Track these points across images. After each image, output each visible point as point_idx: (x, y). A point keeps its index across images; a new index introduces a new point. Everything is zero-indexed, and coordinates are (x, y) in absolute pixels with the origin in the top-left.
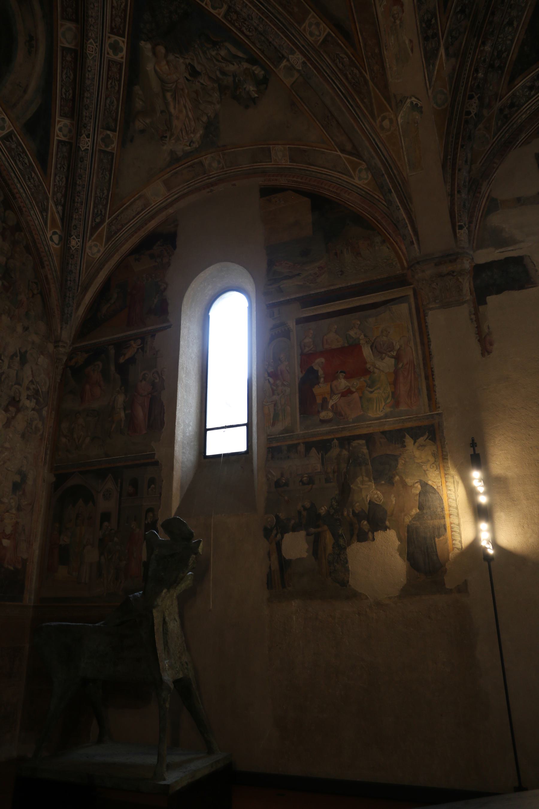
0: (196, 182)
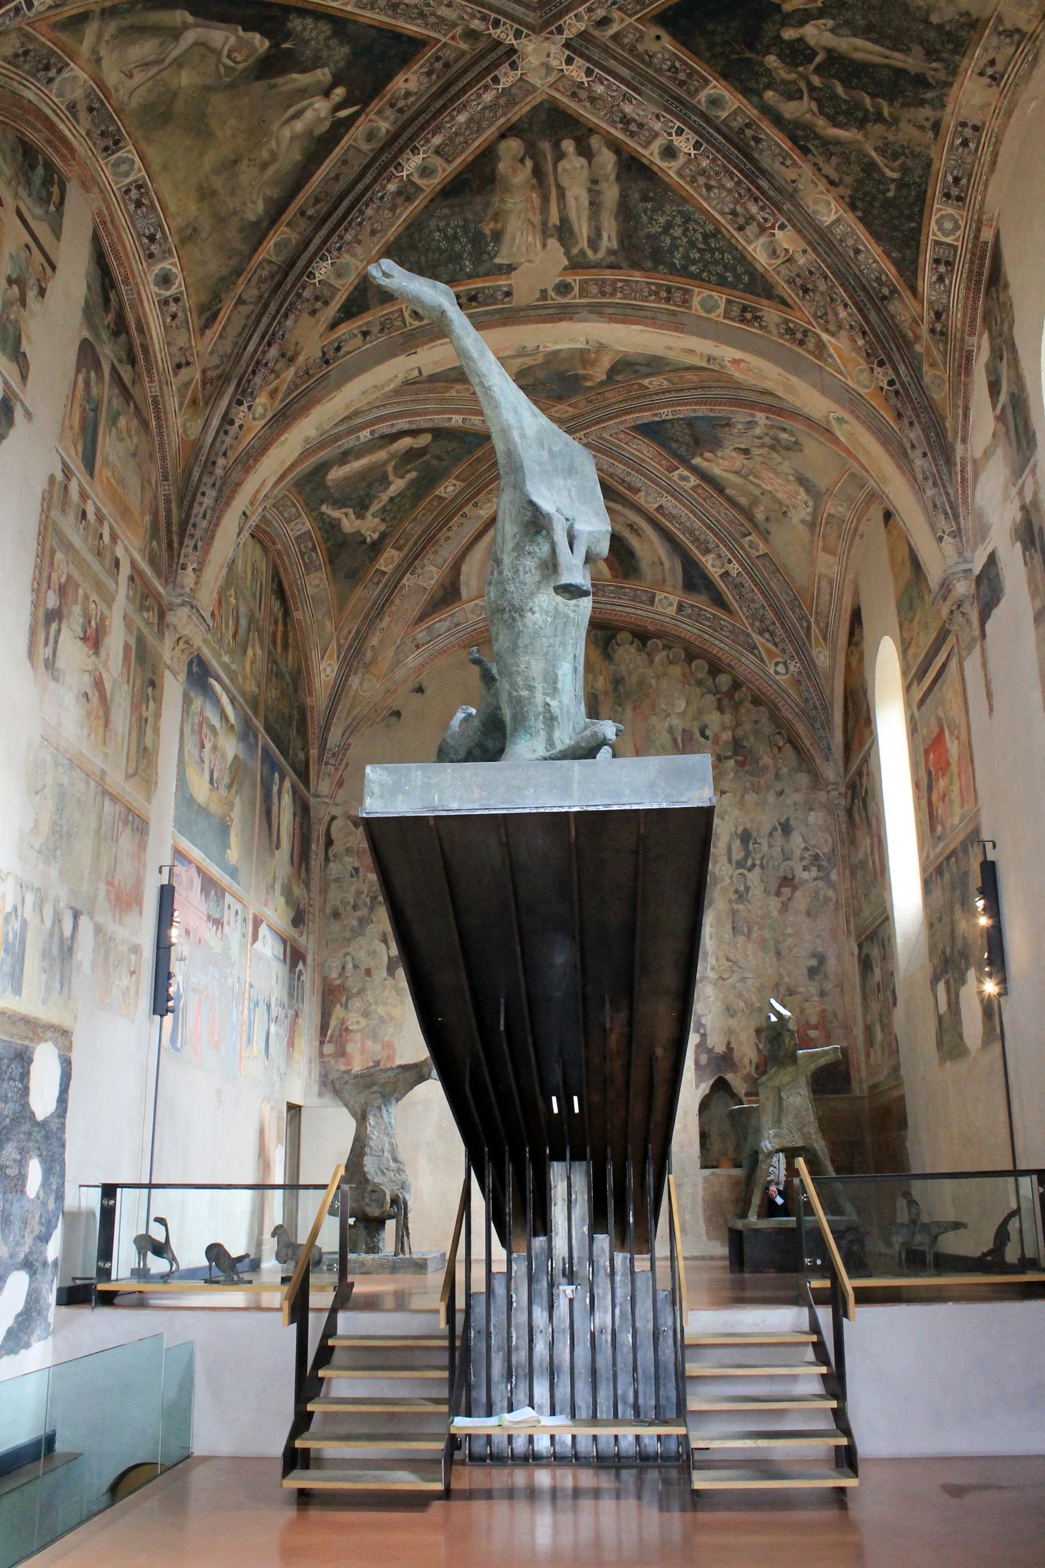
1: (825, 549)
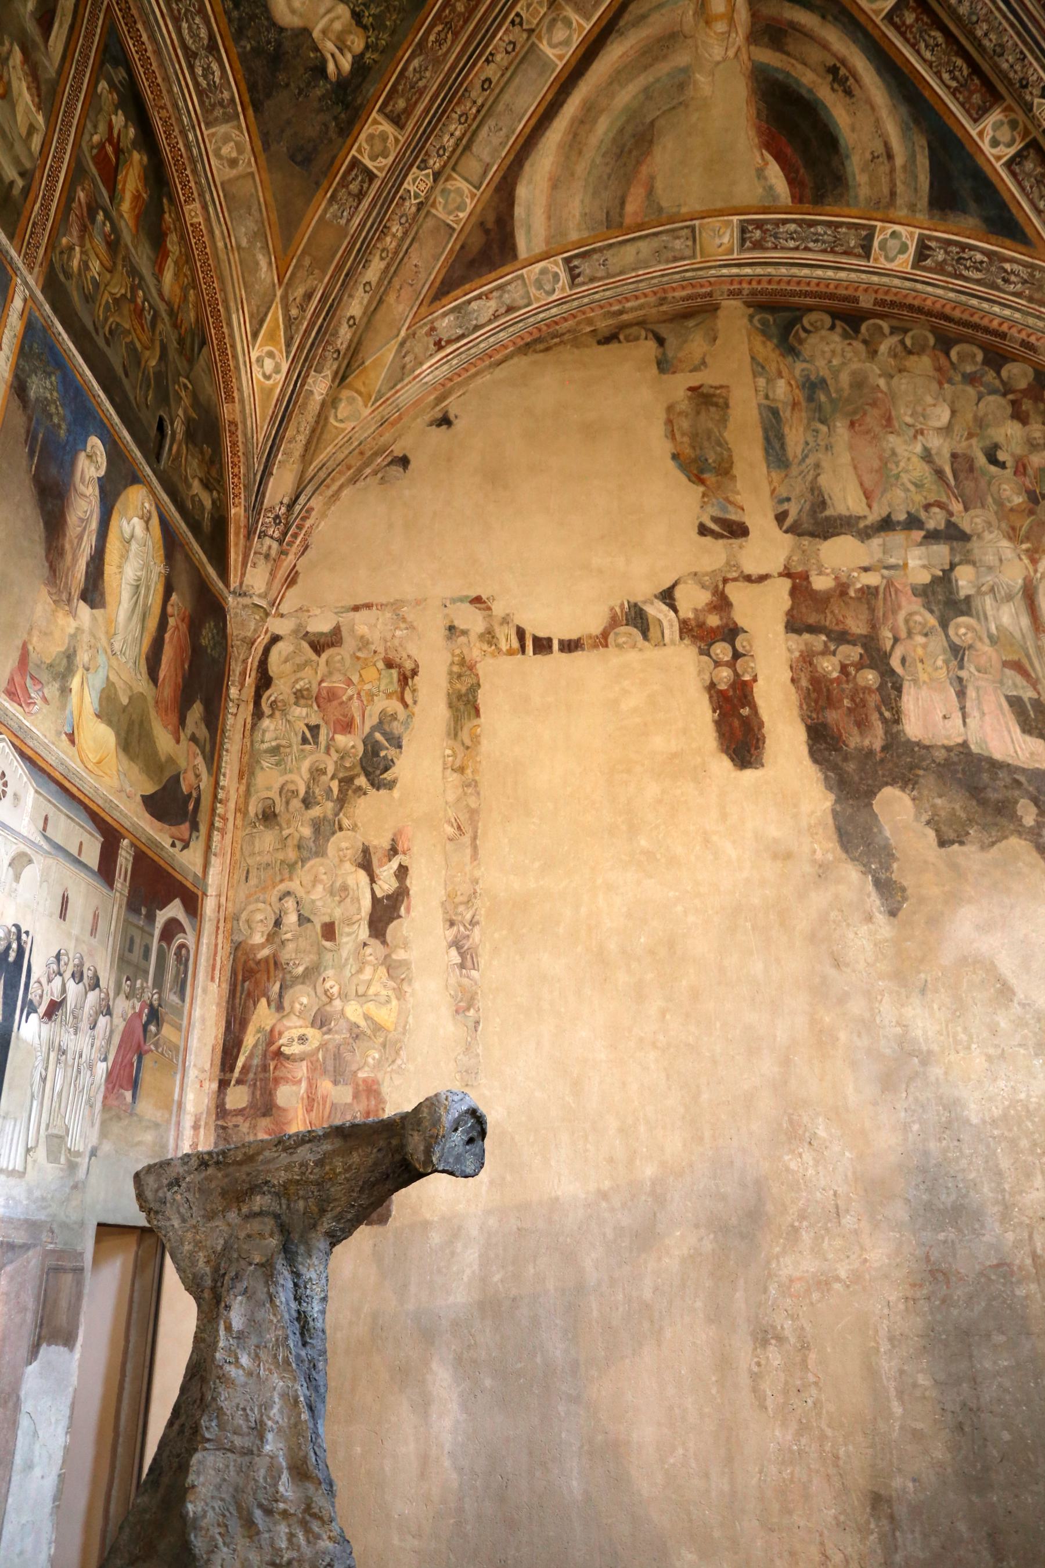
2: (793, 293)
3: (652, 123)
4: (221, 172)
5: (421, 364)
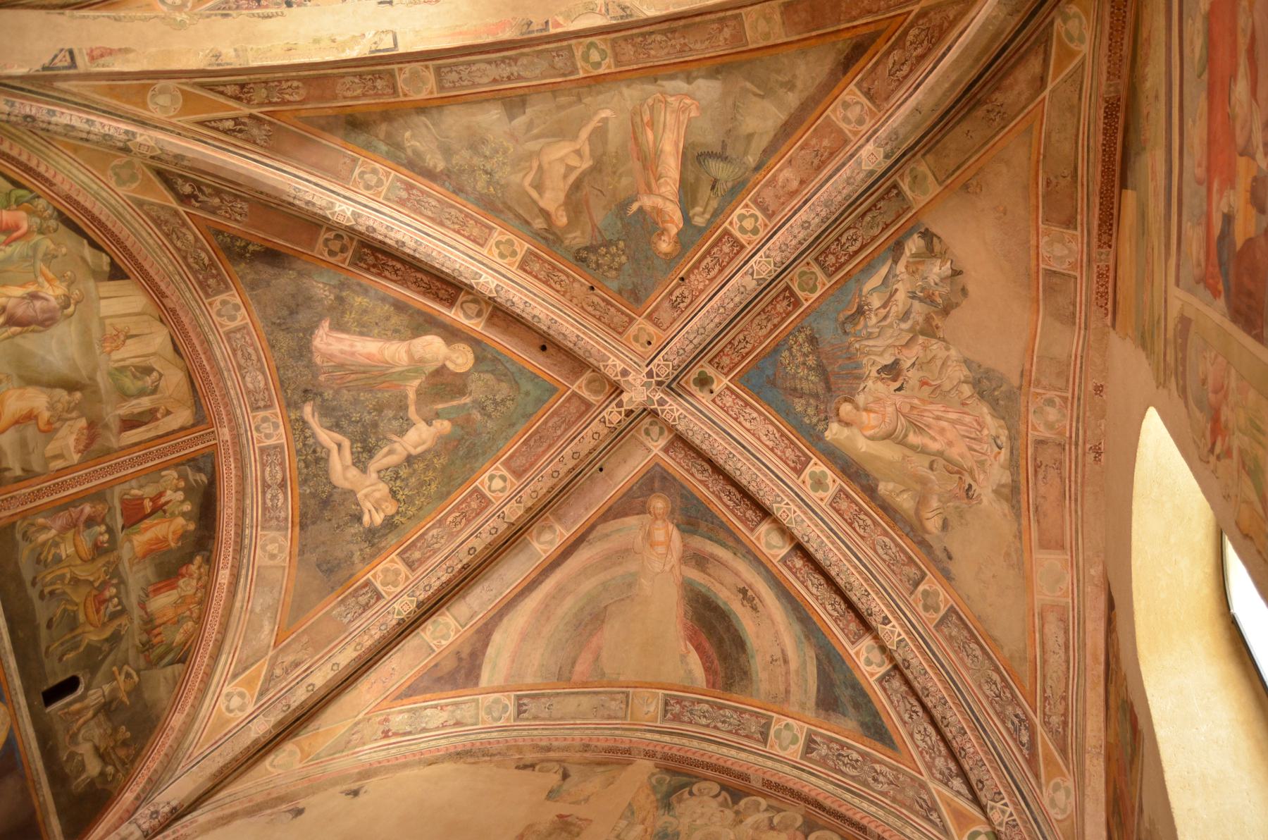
0: (1073, 479)
1: (1044, 545)
2: (698, 764)
3: (606, 607)
4: (261, 558)
5: (364, 744)
